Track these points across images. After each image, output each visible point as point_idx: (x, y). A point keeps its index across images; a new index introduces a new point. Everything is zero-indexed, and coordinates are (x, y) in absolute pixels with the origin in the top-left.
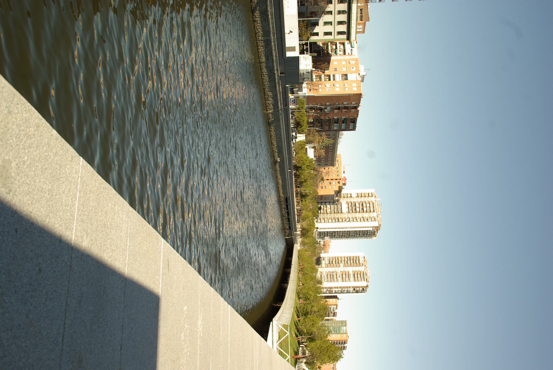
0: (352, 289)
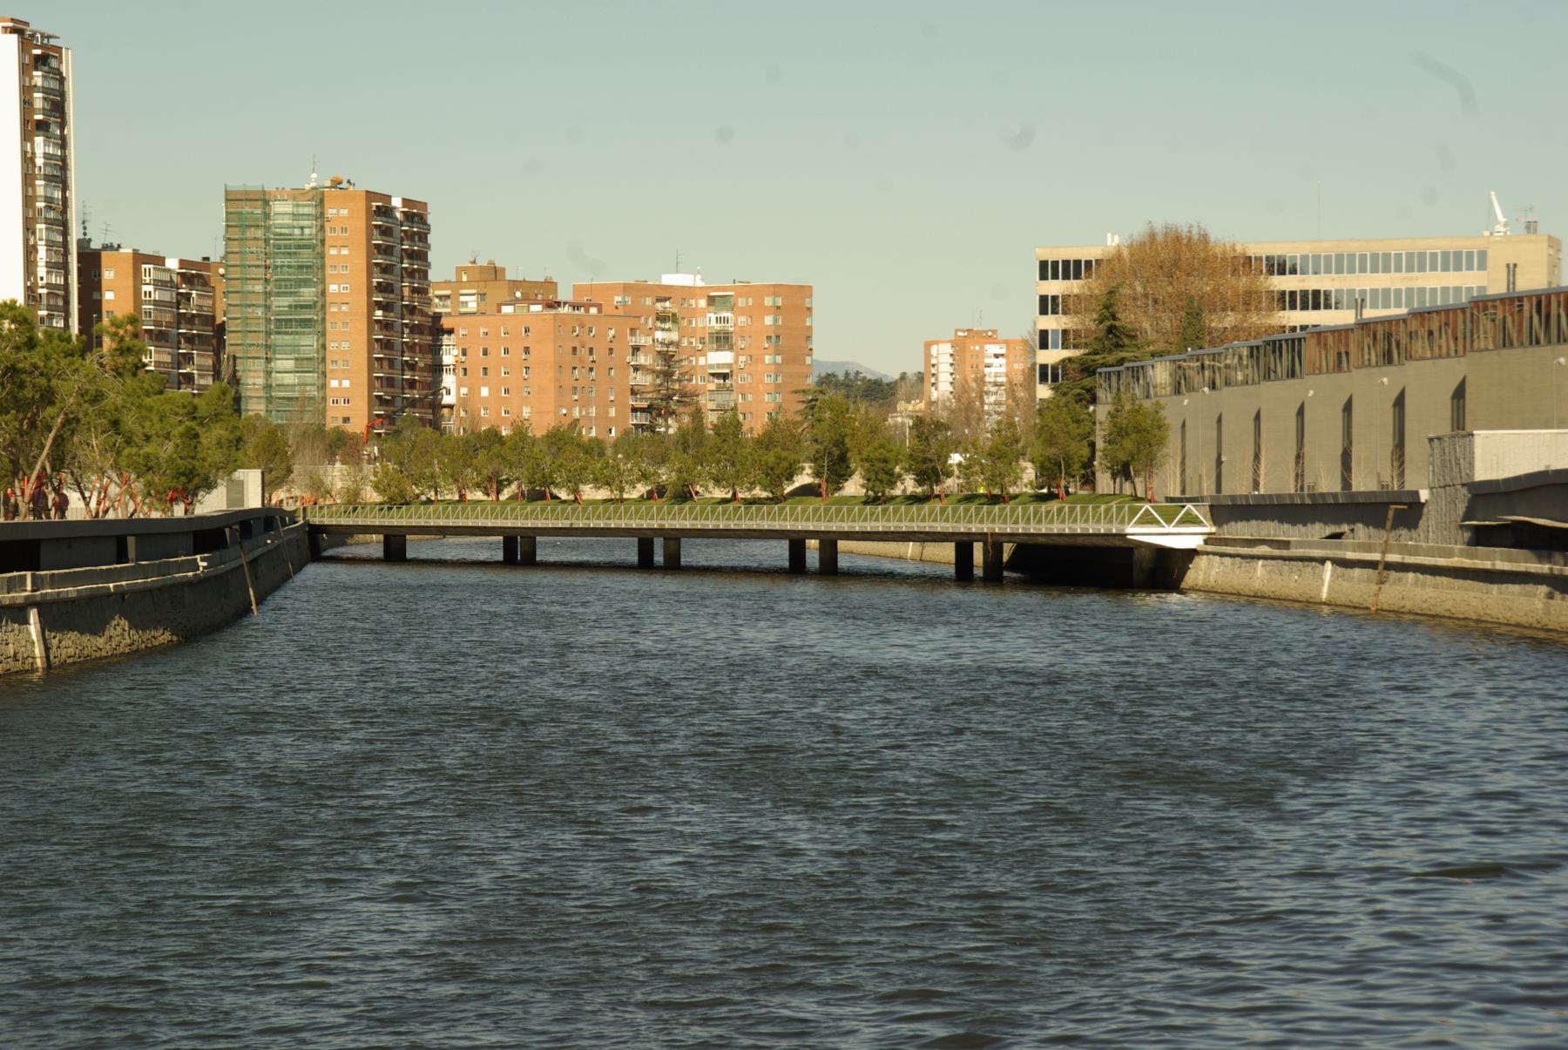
0: (39, 140)
